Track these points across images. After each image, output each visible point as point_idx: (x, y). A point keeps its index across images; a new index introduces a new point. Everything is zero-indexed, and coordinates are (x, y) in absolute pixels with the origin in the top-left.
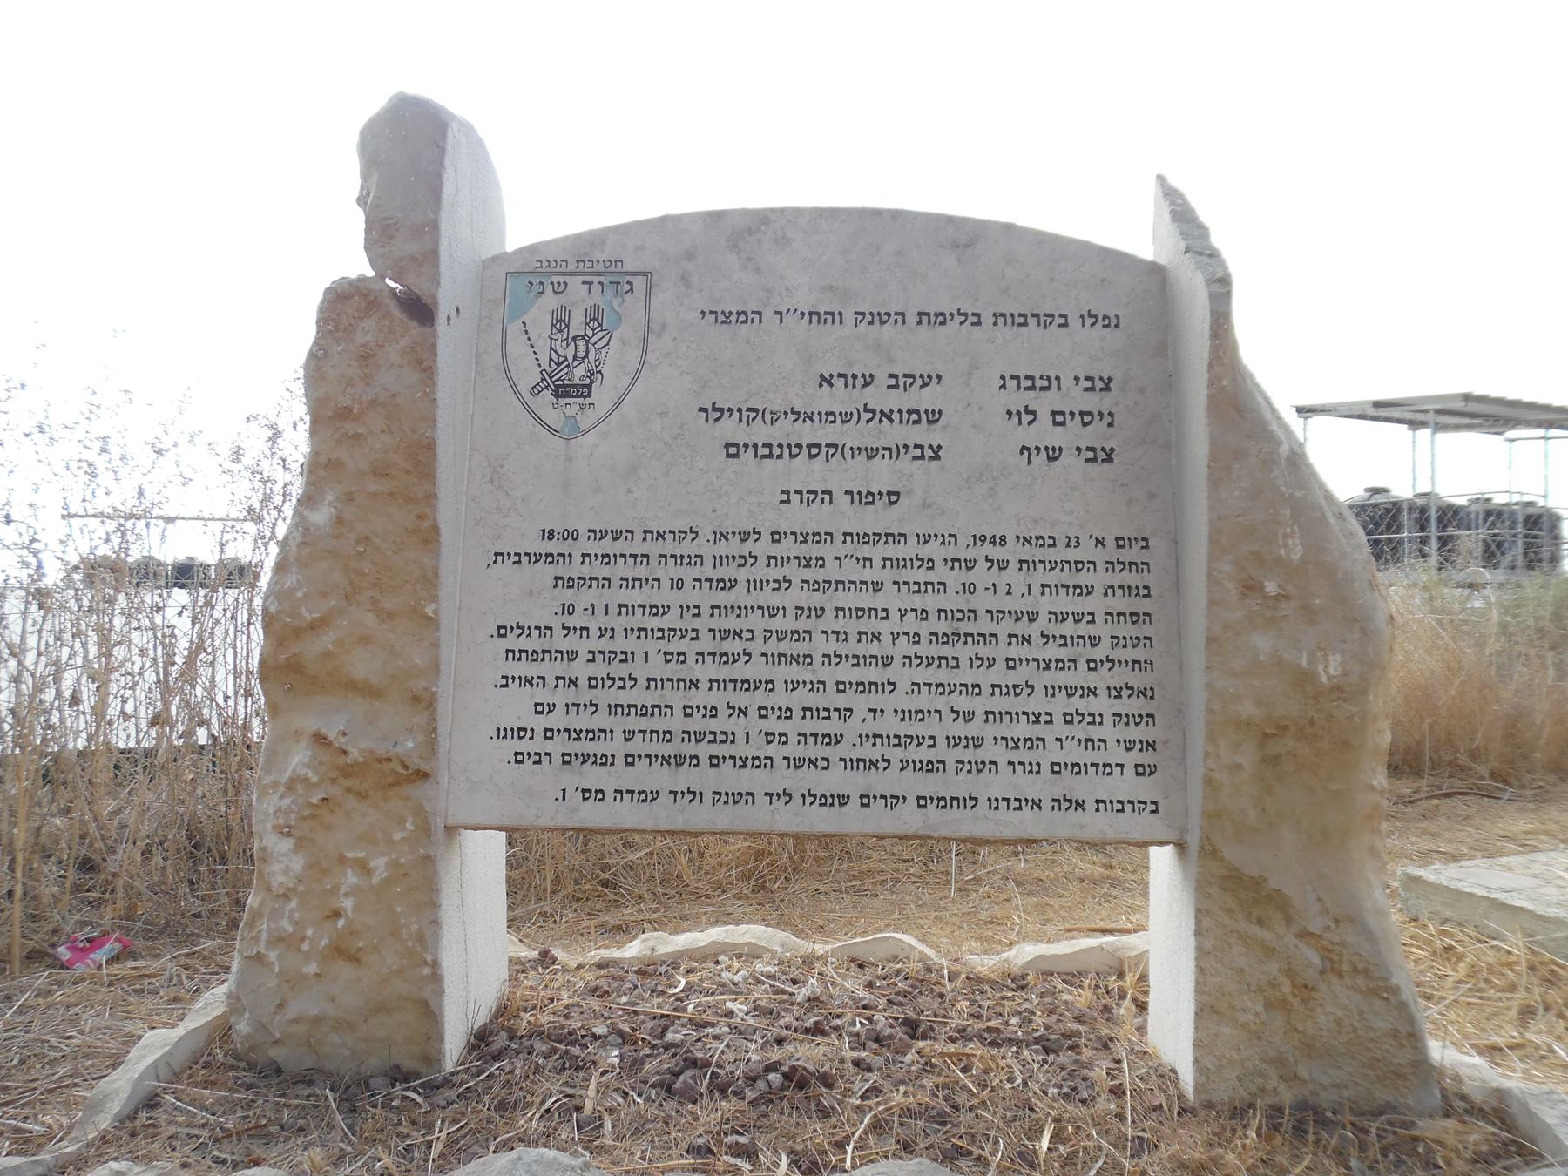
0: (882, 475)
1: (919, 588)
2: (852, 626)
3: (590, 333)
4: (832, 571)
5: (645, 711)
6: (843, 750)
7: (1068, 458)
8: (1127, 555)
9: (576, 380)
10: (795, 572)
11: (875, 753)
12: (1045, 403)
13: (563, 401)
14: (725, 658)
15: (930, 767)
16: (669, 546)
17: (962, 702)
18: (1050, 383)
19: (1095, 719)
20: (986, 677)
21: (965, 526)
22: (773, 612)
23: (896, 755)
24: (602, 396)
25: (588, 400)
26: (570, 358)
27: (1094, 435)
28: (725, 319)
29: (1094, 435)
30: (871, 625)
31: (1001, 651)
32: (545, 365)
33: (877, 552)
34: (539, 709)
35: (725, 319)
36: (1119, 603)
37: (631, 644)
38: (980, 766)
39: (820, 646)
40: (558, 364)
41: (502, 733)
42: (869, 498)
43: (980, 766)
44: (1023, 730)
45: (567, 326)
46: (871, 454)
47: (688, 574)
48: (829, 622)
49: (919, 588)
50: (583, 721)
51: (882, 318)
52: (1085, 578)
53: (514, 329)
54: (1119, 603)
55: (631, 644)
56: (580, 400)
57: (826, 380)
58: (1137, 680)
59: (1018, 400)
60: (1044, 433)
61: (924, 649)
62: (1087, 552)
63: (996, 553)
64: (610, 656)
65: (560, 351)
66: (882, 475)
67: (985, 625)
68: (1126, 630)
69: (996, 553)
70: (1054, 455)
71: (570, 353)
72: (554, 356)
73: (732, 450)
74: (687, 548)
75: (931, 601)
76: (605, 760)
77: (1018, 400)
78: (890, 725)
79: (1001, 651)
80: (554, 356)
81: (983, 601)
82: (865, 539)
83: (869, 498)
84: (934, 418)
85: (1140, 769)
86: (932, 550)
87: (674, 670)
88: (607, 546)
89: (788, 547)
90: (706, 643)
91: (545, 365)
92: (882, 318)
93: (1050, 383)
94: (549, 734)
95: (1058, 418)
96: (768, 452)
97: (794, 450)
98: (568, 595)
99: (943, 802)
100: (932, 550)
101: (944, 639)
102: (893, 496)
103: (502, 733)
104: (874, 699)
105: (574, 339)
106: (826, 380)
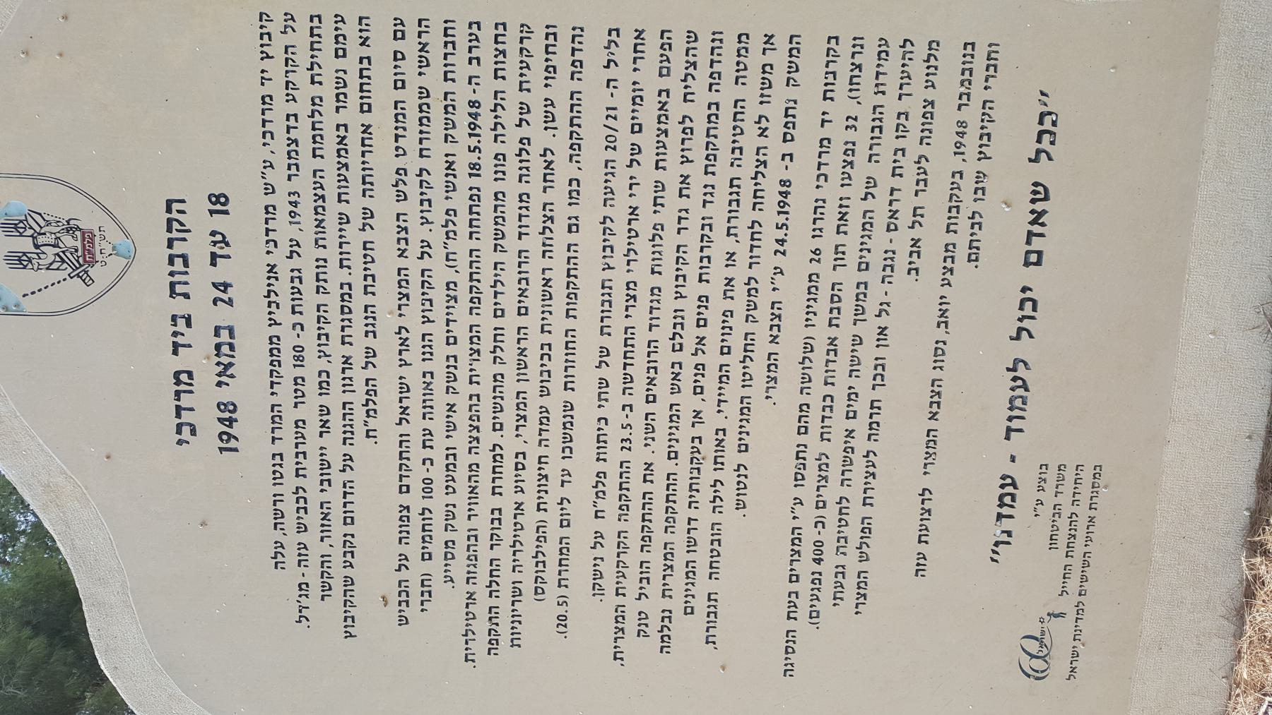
3: (30, 232)
9: (79, 244)
13: (98, 257)
24: (89, 220)
25: (97, 233)
26: (57, 250)
32: (65, 274)
40: (63, 261)
45: (24, 254)
53: (29, 305)
56: (97, 239)
65: (51, 258)
71: (50, 251)
72: (55, 266)
80: (55, 266)
91: (65, 274)
105: (37, 246)
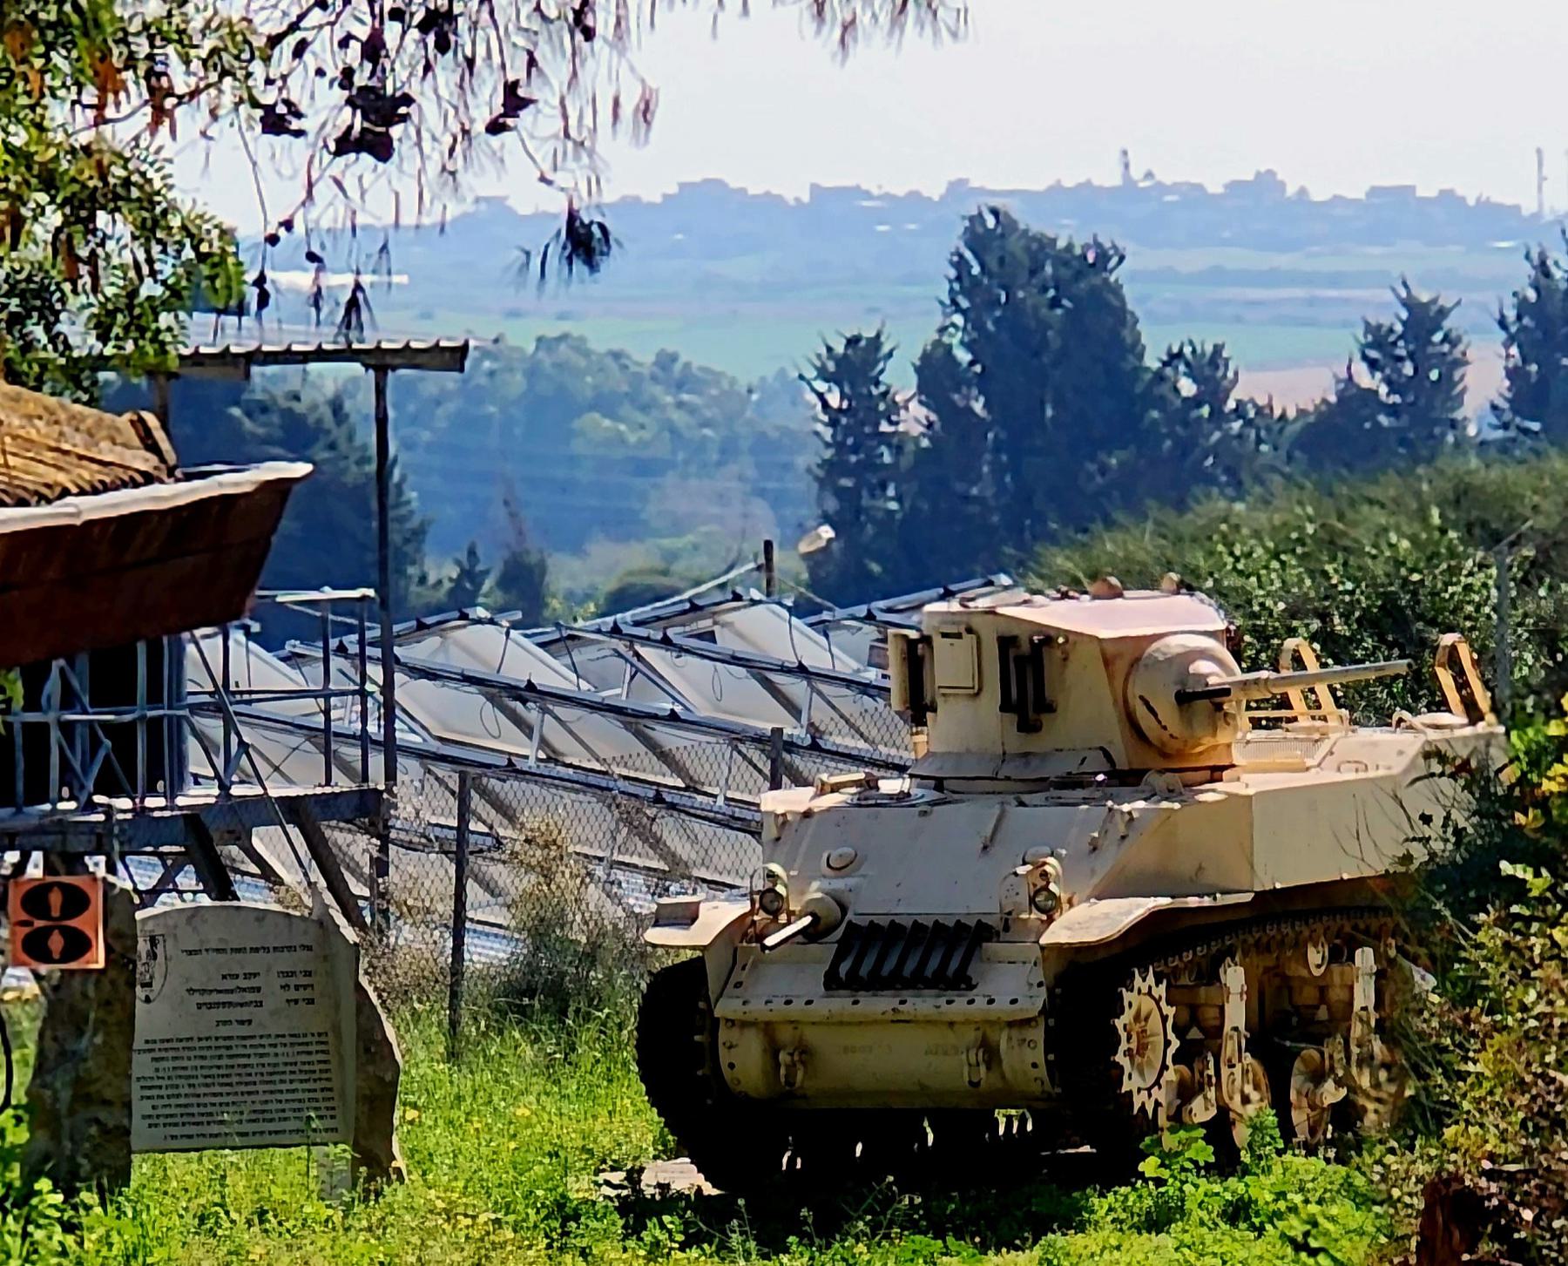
0: (244, 1013)
1: (262, 1055)
2: (243, 1071)
4: (234, 1051)
5: (186, 1106)
6: (245, 1117)
7: (301, 1003)
8: (323, 1039)
10: (223, 1052)
11: (254, 1116)
12: (292, 981)
14: (207, 1085)
15: (271, 1120)
16: (184, 1044)
17: (279, 1097)
18: (293, 974)
19: (317, 1100)
20: (283, 1087)
21: (273, 1032)
22: (219, 1067)
23: (261, 1116)
24: (156, 985)
27: (307, 994)
28: (190, 953)
29: (307, 994)
30: (249, 1070)
31: (287, 1077)
33: (248, 1043)
34: (154, 1107)
35: (190, 953)
36: (321, 1057)
37: (178, 1082)
38: (285, 1119)
39: (235, 1079)
41: (144, 1117)
42: (241, 1022)
43: (285, 1119)
44: (296, 1105)
46: (242, 1005)
47: (192, 1054)
48: (237, 1070)
49: (262, 1055)
50: (167, 1111)
51: (238, 950)
52: (310, 1048)
54: (321, 1057)
55: (178, 1082)
57: (224, 977)
58: (328, 1085)
59: (284, 981)
60: (293, 994)
61: (267, 1078)
62: (309, 1039)
63: (283, 1040)
64: (172, 1086)
66: (244, 1013)
67: (281, 1068)
68: (323, 1066)
69: (283, 1040)
70: (296, 1002)
73: (199, 1006)
74: (190, 1044)
75: (265, 1060)
76: (176, 1125)
77: (284, 981)
78: (258, 1107)
79: (287, 1077)
81: (281, 1060)
82: (244, 1038)
83: (241, 1022)
84: (259, 989)
85: (333, 1117)
86: (263, 1042)
87: (191, 1091)
88: (166, 1045)
89: (221, 1043)
90: (201, 1080)
92: (238, 950)
93: (293, 974)
94: (158, 1116)
95: (297, 988)
96: (210, 1006)
97: (217, 1005)
98: (157, 1065)
99: (276, 1132)
100: (263, 1042)
101: (271, 1074)
102: (250, 1022)
103: (144, 1117)
104: (253, 1098)
106: (224, 977)
